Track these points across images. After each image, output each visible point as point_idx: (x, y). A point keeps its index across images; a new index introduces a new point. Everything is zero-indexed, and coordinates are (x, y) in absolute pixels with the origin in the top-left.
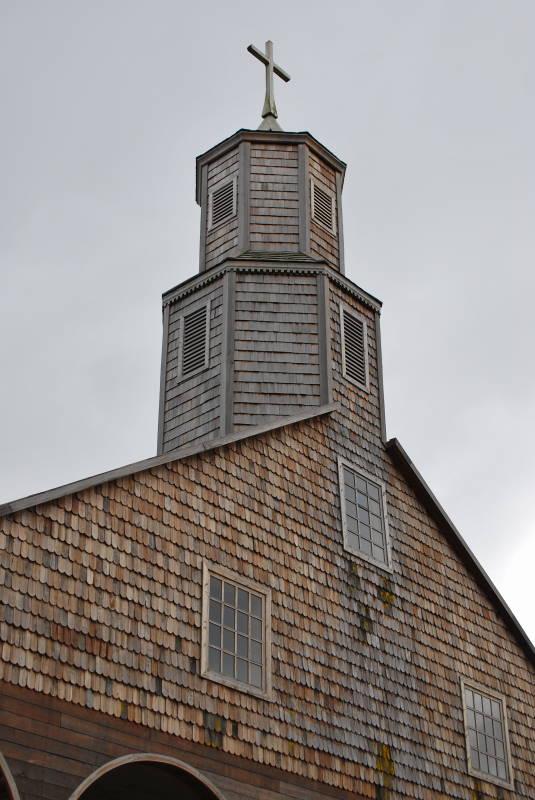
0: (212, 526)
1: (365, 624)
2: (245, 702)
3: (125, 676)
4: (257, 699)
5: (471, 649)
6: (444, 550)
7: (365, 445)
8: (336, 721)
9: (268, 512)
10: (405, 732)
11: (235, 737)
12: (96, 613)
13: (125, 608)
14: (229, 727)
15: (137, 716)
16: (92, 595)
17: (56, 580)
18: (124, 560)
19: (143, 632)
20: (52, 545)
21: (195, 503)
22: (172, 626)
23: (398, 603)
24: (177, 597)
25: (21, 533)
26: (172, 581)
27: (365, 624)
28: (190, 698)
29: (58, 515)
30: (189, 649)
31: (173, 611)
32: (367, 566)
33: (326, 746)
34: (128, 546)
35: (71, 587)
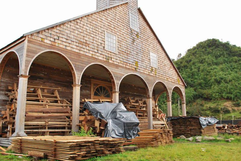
0: (107, 23)
1: (134, 40)
2: (113, 54)
3: (92, 50)
4: (115, 54)
5: (152, 45)
6: (148, 28)
7: (134, 8)
8: (128, 57)
9: (116, 21)
10: (140, 59)
11: (111, 60)
12: (86, 39)
13: (91, 38)
14: (110, 58)
15: (94, 56)
16: (85, 36)
17: (79, 33)
18: (91, 29)
19: (95, 42)
20: (78, 27)
21: (103, 19)
22: (100, 41)
23: (139, 37)
24: (101, 36)
25: (72, 24)
26: (100, 33)
27: (134, 40)
28: (103, 53)
29: (78, 21)
30: (103, 45)
31: (100, 38)
32: (134, 31)
33: (127, 62)
34: (91, 27)
35: (82, 34)
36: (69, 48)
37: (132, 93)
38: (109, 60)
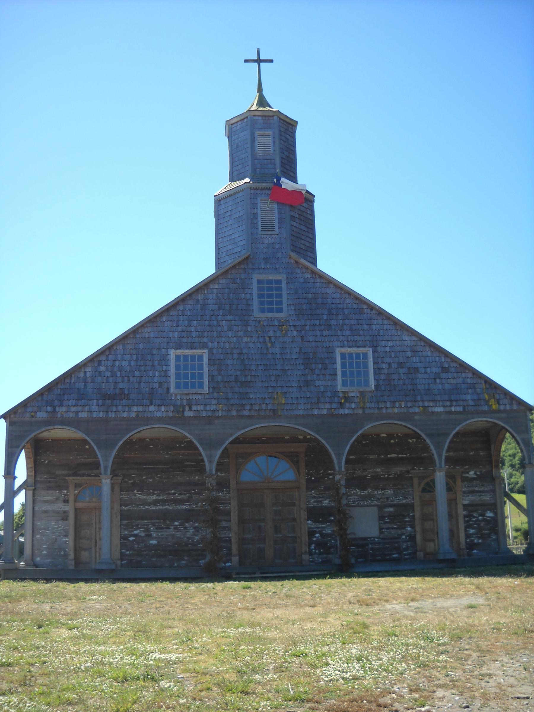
5: (348, 333)
14: (187, 408)
36: (83, 415)
37: (379, 455)
38: (185, 413)
